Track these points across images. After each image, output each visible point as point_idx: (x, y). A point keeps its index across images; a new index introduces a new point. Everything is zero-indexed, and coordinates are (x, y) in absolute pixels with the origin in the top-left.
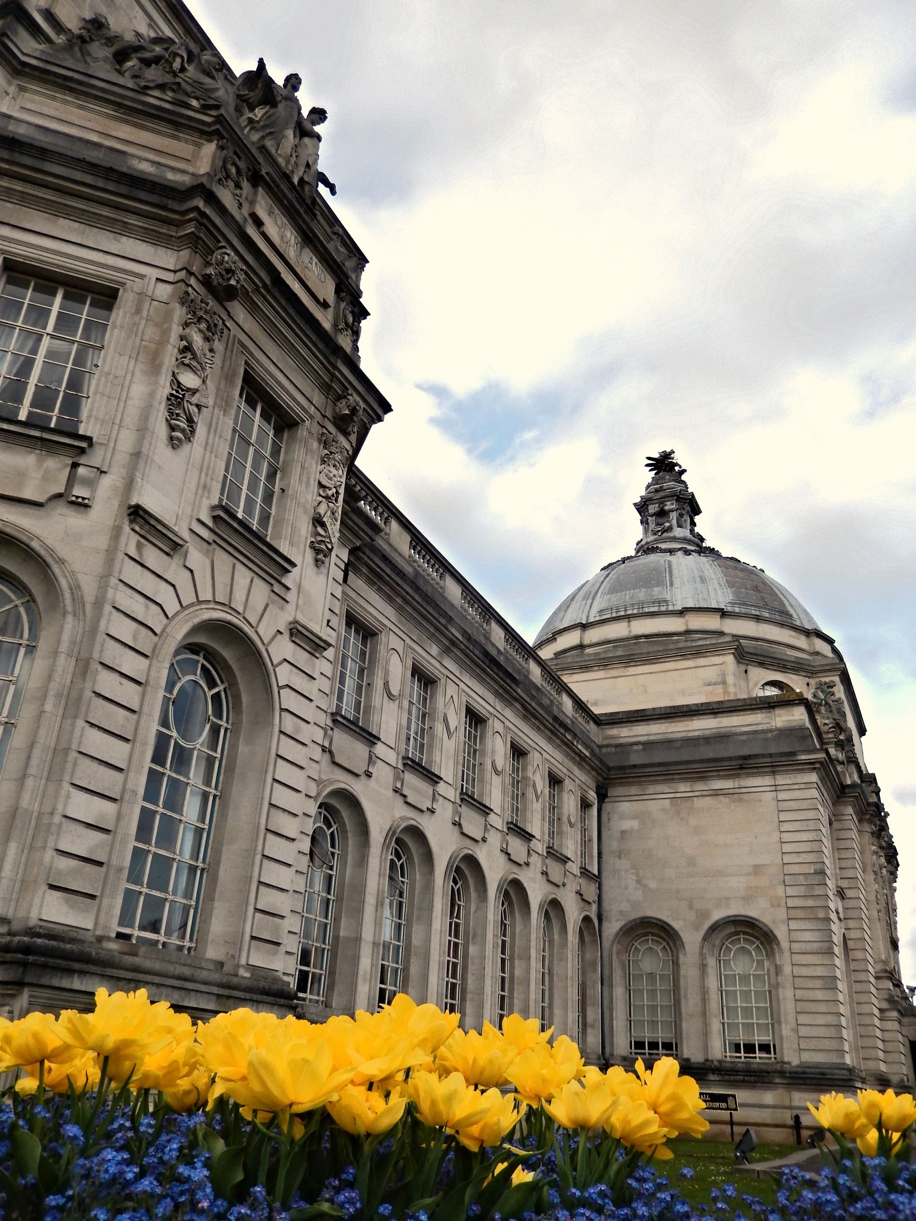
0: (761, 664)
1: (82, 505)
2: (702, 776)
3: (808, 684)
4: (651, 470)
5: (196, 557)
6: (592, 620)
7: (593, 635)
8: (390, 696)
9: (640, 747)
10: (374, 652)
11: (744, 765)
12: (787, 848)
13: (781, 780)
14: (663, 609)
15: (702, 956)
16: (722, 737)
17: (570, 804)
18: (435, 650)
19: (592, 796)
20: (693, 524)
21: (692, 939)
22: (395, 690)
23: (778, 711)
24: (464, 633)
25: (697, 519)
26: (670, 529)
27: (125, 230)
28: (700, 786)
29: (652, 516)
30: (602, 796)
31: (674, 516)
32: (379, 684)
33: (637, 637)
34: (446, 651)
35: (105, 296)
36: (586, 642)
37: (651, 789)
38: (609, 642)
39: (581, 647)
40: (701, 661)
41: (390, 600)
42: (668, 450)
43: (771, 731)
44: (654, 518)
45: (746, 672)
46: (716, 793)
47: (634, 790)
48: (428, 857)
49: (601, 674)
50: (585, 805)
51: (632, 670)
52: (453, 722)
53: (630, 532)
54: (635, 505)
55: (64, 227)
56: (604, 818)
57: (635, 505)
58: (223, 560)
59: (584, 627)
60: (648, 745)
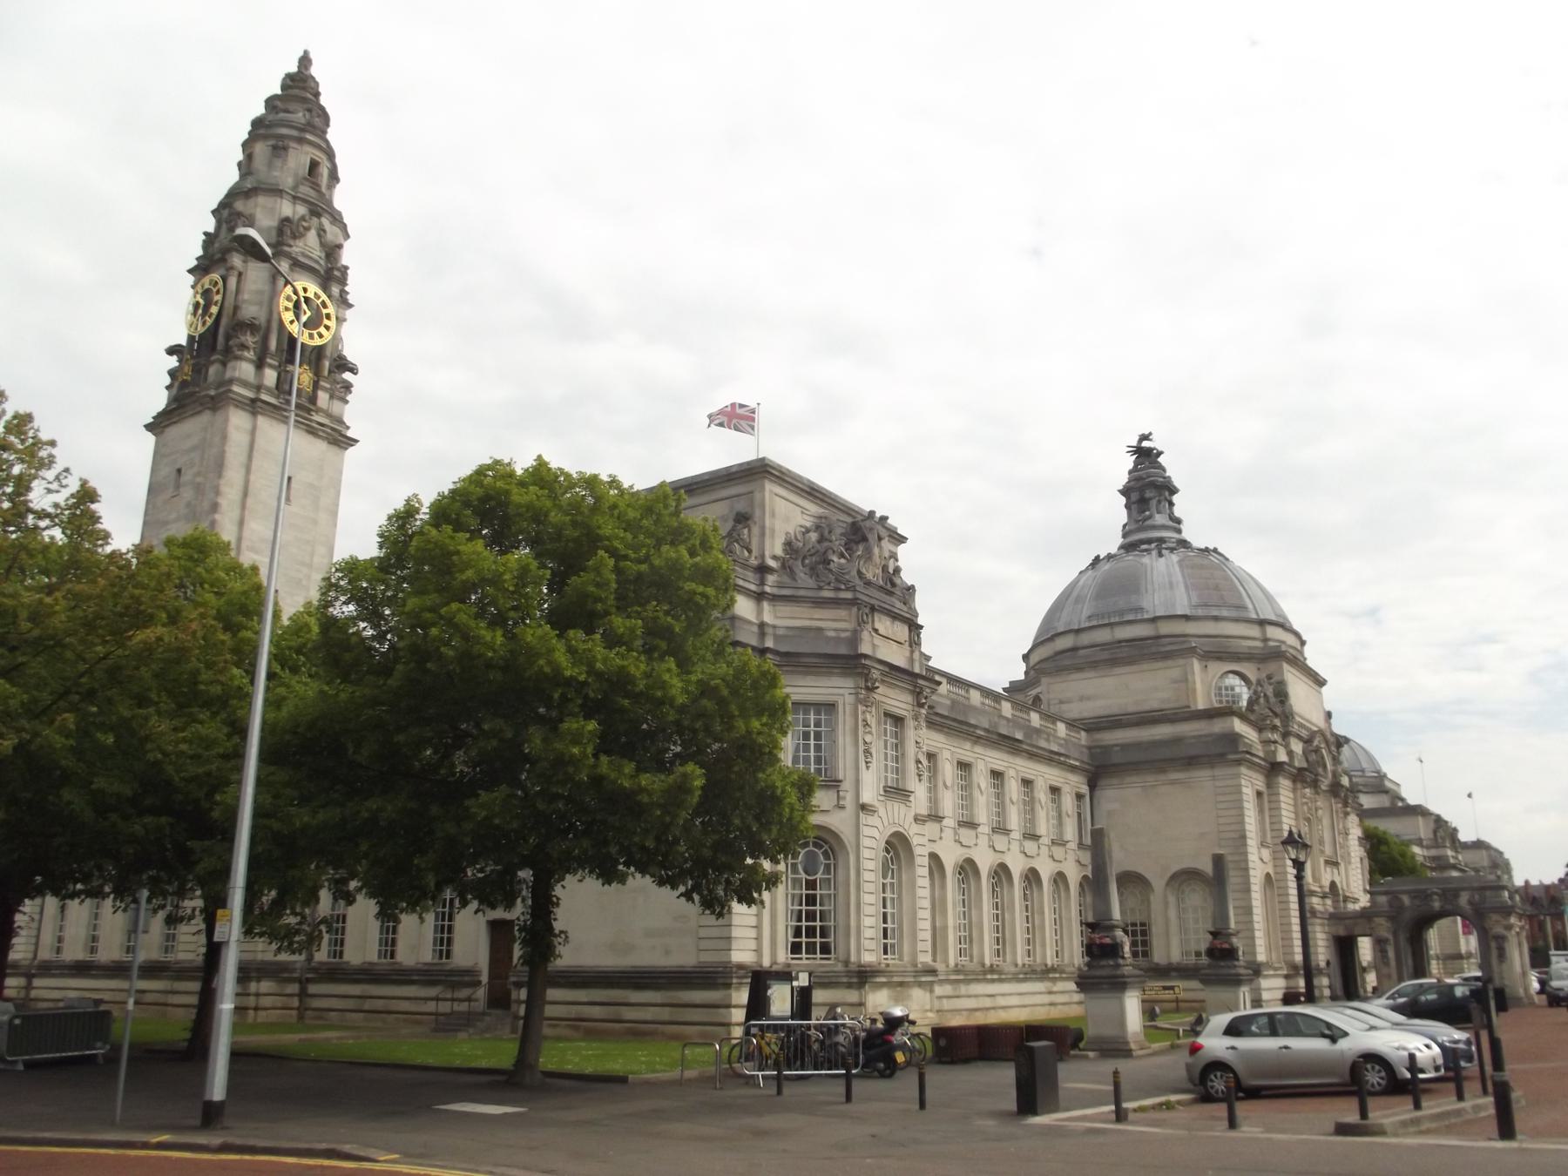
0: (1220, 659)
1: (843, 808)
2: (1163, 771)
5: (882, 811)
7: (1085, 639)
11: (1191, 762)
12: (1222, 821)
15: (1165, 897)
16: (1177, 741)
17: (1068, 802)
18: (968, 745)
19: (1085, 789)
20: (1171, 504)
21: (1158, 884)
22: (949, 783)
24: (986, 730)
25: (1175, 498)
26: (1150, 517)
27: (830, 674)
28: (1162, 777)
30: (1093, 786)
31: (1154, 503)
32: (940, 784)
34: (975, 743)
35: (831, 707)
37: (1128, 779)
39: (1074, 649)
40: (1170, 663)
41: (940, 731)
43: (1210, 735)
46: (1173, 783)
47: (1115, 781)
48: (977, 872)
50: (1079, 797)
52: (983, 786)
53: (1116, 513)
55: (810, 680)
59: (1078, 631)
60: (1125, 747)
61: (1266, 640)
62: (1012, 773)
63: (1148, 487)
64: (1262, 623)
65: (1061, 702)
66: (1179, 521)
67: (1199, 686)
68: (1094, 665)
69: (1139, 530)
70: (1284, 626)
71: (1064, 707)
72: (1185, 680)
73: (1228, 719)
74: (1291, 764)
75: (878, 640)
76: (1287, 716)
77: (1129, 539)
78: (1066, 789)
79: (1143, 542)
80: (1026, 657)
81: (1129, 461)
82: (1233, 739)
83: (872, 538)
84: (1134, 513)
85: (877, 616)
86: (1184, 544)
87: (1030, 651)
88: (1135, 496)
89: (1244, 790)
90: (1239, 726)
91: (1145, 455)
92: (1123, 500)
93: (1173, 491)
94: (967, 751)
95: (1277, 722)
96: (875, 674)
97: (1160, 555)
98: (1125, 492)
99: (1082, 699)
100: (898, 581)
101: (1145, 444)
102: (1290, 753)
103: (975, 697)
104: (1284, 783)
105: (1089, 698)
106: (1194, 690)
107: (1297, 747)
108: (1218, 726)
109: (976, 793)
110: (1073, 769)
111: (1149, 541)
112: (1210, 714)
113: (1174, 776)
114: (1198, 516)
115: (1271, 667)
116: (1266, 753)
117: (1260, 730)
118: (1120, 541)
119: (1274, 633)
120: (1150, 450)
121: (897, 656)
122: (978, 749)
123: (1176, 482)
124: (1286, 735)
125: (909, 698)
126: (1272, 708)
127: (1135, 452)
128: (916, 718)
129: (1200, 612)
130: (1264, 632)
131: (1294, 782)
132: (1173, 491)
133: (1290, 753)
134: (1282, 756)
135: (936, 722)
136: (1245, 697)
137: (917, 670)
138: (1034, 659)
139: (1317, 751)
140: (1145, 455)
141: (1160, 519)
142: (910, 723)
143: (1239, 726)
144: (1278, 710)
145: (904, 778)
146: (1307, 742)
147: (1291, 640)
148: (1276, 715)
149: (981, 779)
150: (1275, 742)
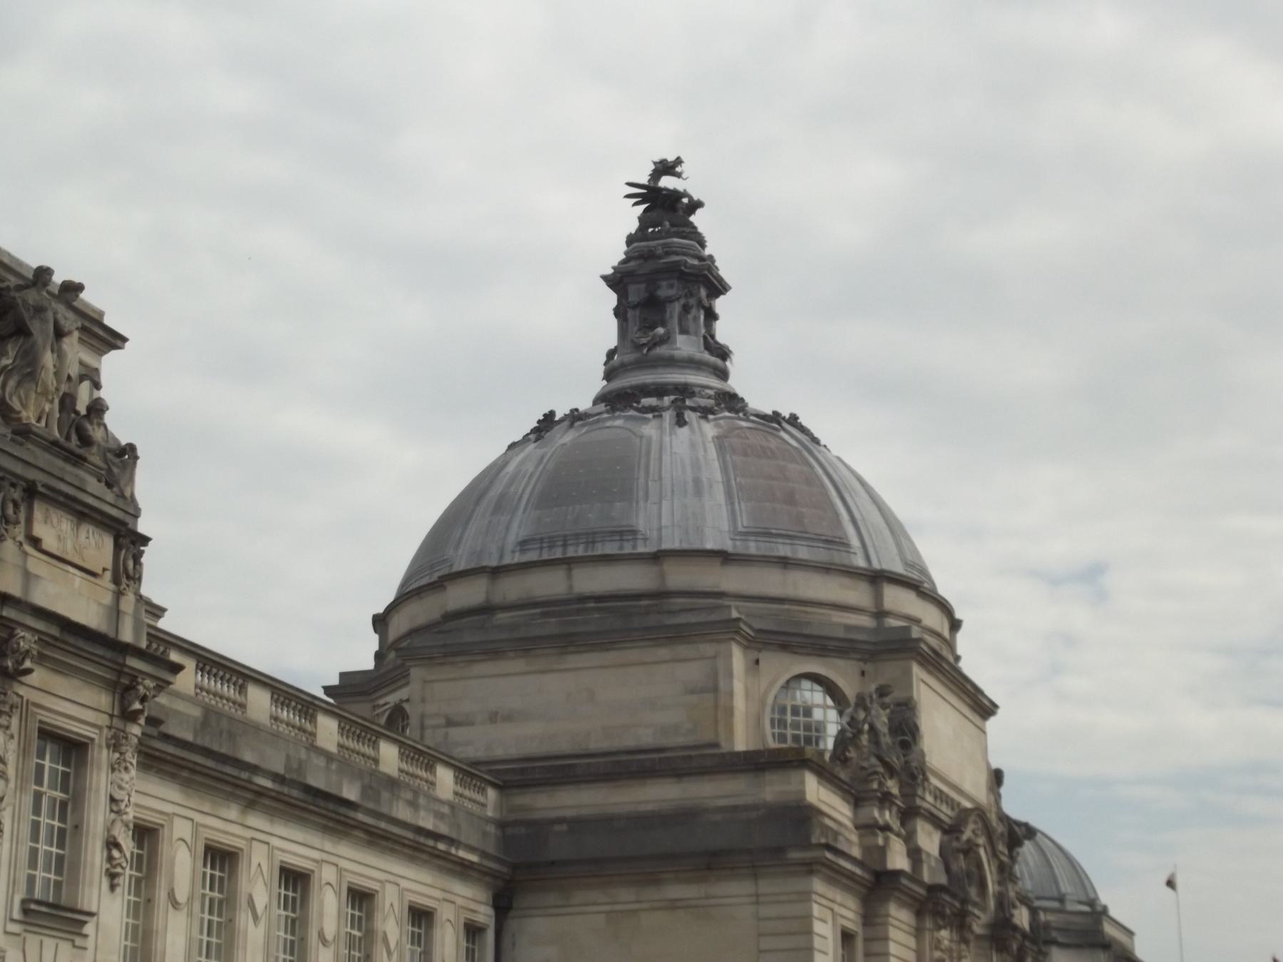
0: (785, 647)
2: (654, 880)
3: (863, 673)
4: (635, 204)
6: (507, 560)
7: (512, 589)
8: (175, 904)
9: (564, 827)
10: (153, 853)
11: (712, 862)
13: (765, 886)
14: (628, 549)
16: (685, 816)
18: (233, 812)
19: (485, 915)
20: (711, 316)
22: (182, 896)
23: (769, 777)
24: (276, 777)
25: (720, 304)
26: (666, 340)
29: (634, 307)
30: (503, 906)
32: (161, 895)
33: (582, 599)
34: (250, 805)
36: (497, 599)
38: (535, 604)
39: (486, 610)
40: (683, 650)
41: (173, 777)
42: (671, 158)
43: (755, 807)
44: (637, 312)
45: (757, 662)
46: (673, 905)
49: (519, 665)
50: (473, 931)
51: (574, 660)
52: (261, 900)
53: (594, 325)
54: (605, 278)
56: (506, 942)
57: (605, 278)
58: (33, 941)
59: (496, 572)
60: (578, 825)
61: (880, 614)
62: (328, 874)
63: (665, 274)
64: (877, 578)
65: (450, 723)
66: (724, 353)
67: (739, 703)
68: (526, 646)
69: (640, 365)
70: (920, 587)
71: (455, 733)
72: (713, 689)
73: (794, 775)
74: (915, 877)
75: (37, 564)
76: (914, 774)
77: (619, 383)
78: (445, 914)
79: (646, 390)
80: (380, 622)
81: (630, 217)
82: (802, 816)
83: (40, 331)
84: (633, 328)
85: (39, 511)
86: (731, 401)
87: (392, 608)
88: (637, 292)
89: (818, 927)
90: (815, 791)
91: (664, 207)
92: (612, 299)
93: (718, 288)
94: (229, 823)
95: (893, 786)
96: (26, 640)
97: (681, 422)
98: (616, 281)
99: (493, 717)
100: (97, 434)
101: (667, 182)
102: (915, 854)
103: (259, 702)
104: (899, 918)
105: (509, 718)
106: (730, 711)
107: (929, 840)
108: (772, 789)
109: (243, 919)
110: (462, 870)
111: (660, 391)
112: (758, 763)
113: (675, 891)
114: (763, 345)
115: (888, 671)
116: (867, 849)
117: (857, 800)
118: (597, 384)
119: (899, 600)
120: (676, 196)
121: (83, 604)
122: (256, 820)
123: (725, 270)
124: (909, 814)
125: (103, 700)
126: (884, 758)
127: (642, 199)
128: (115, 744)
129: (753, 548)
130: (878, 597)
131: (919, 914)
132: (718, 288)
133: (915, 854)
134: (898, 860)
135: (164, 757)
136: (832, 730)
137: (127, 636)
138: (399, 625)
139: (969, 850)
140: (664, 207)
141: (685, 346)
142: (101, 756)
143: (815, 791)
144: (896, 761)
145: (74, 881)
146: (950, 830)
147: (931, 617)
148: (891, 771)
149: (258, 886)
150: (886, 828)
